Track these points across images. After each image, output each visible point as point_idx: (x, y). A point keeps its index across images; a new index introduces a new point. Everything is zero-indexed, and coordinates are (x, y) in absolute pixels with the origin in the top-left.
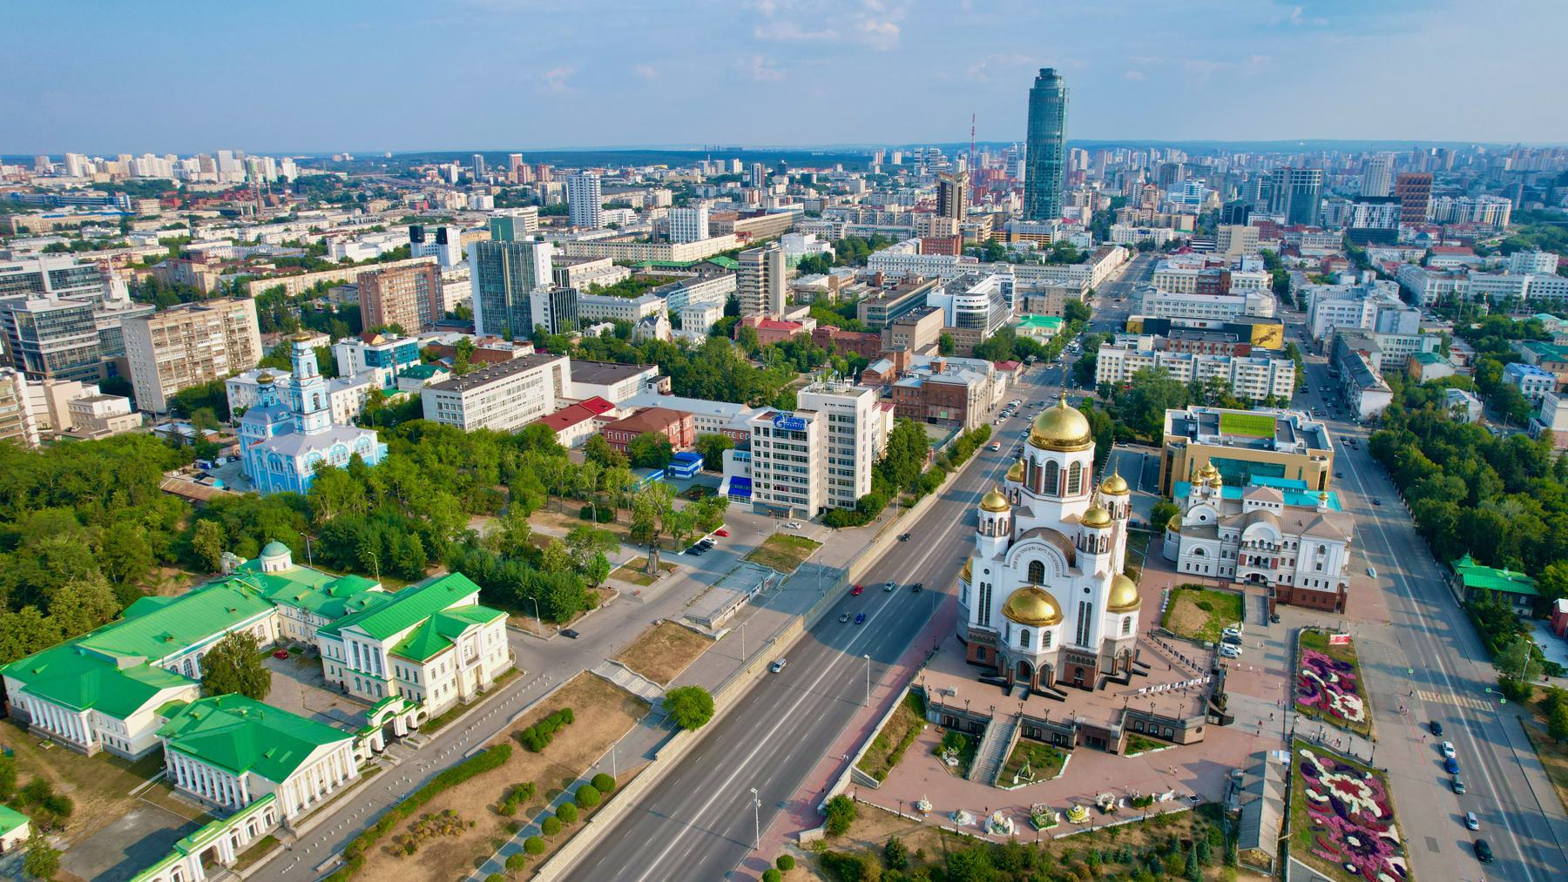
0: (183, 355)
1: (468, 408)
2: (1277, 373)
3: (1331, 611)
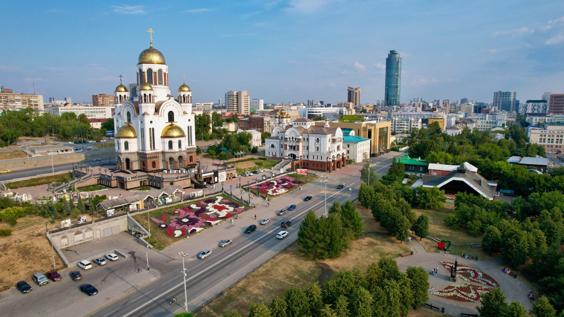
2: (412, 124)
3: (324, 171)
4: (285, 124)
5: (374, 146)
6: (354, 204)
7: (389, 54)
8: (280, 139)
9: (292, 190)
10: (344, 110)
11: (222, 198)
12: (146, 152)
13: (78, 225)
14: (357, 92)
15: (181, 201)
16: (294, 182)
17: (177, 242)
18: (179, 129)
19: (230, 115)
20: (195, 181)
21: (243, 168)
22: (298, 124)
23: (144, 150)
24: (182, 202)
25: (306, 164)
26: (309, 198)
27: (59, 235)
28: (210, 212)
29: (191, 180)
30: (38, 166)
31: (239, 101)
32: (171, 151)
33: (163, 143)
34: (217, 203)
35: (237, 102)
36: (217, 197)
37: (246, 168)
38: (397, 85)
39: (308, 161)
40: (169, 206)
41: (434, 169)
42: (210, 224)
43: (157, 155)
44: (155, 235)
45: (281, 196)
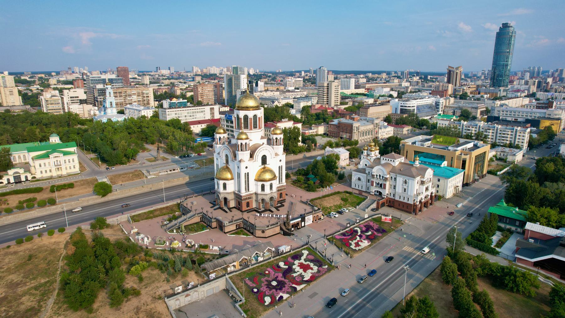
0: (123, 101)
1: (169, 115)
2: (518, 134)
3: (410, 213)
4: (373, 158)
5: (468, 175)
6: (436, 274)
7: (500, 27)
8: (367, 174)
9: (374, 243)
10: (441, 101)
11: (307, 252)
12: (242, 195)
13: (187, 290)
14: (458, 71)
15: (270, 258)
16: (378, 230)
17: (267, 312)
18: (271, 171)
19: (319, 108)
20: (284, 228)
21: (328, 206)
22: (386, 159)
23: (240, 192)
24: (272, 259)
25: (392, 203)
26: (390, 259)
27: (174, 299)
28: (296, 272)
29: (280, 227)
30: (153, 189)
31: (329, 92)
32: (263, 193)
33: (257, 185)
34: (302, 261)
35: (328, 93)
36: (303, 252)
37: (332, 205)
38: (507, 63)
39: (394, 199)
40: (260, 264)
41: (532, 229)
42: (295, 288)
43: (251, 196)
44: (249, 301)
45: (363, 251)
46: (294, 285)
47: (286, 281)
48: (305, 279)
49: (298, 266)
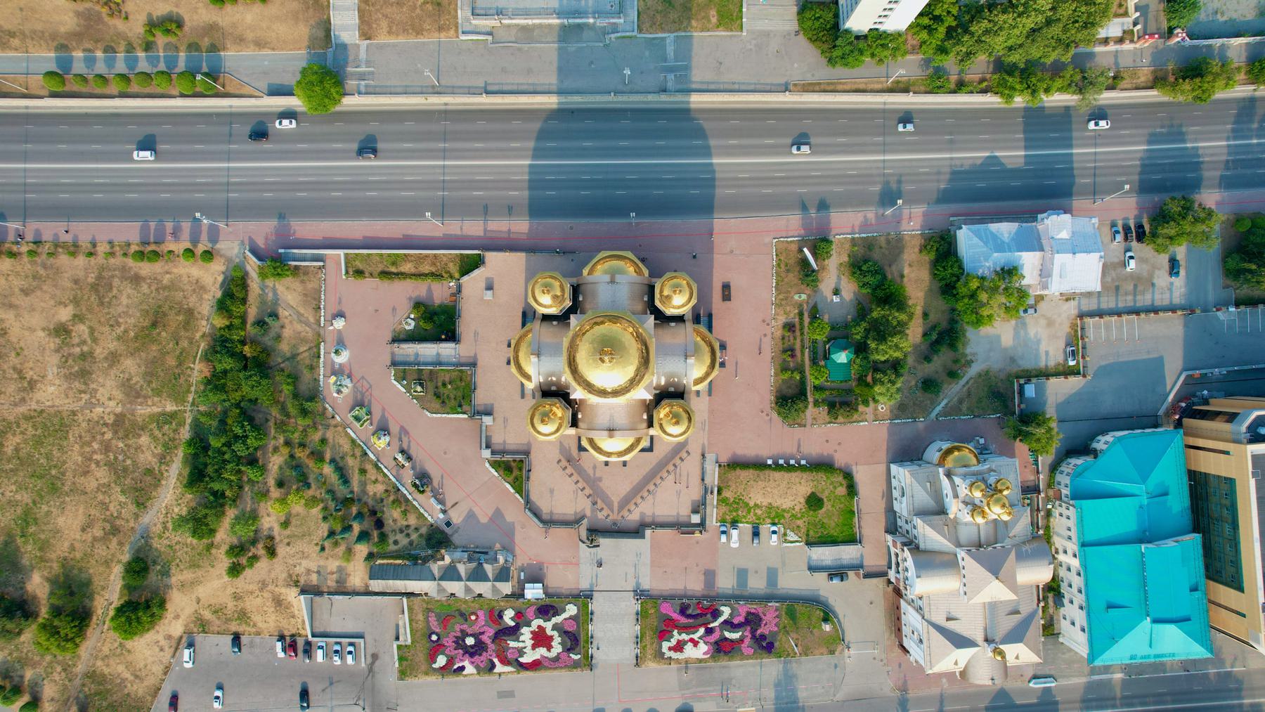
28: (519, 641)
42: (493, 666)
46: (496, 660)
47: (492, 647)
48: (521, 660)
49: (532, 632)
